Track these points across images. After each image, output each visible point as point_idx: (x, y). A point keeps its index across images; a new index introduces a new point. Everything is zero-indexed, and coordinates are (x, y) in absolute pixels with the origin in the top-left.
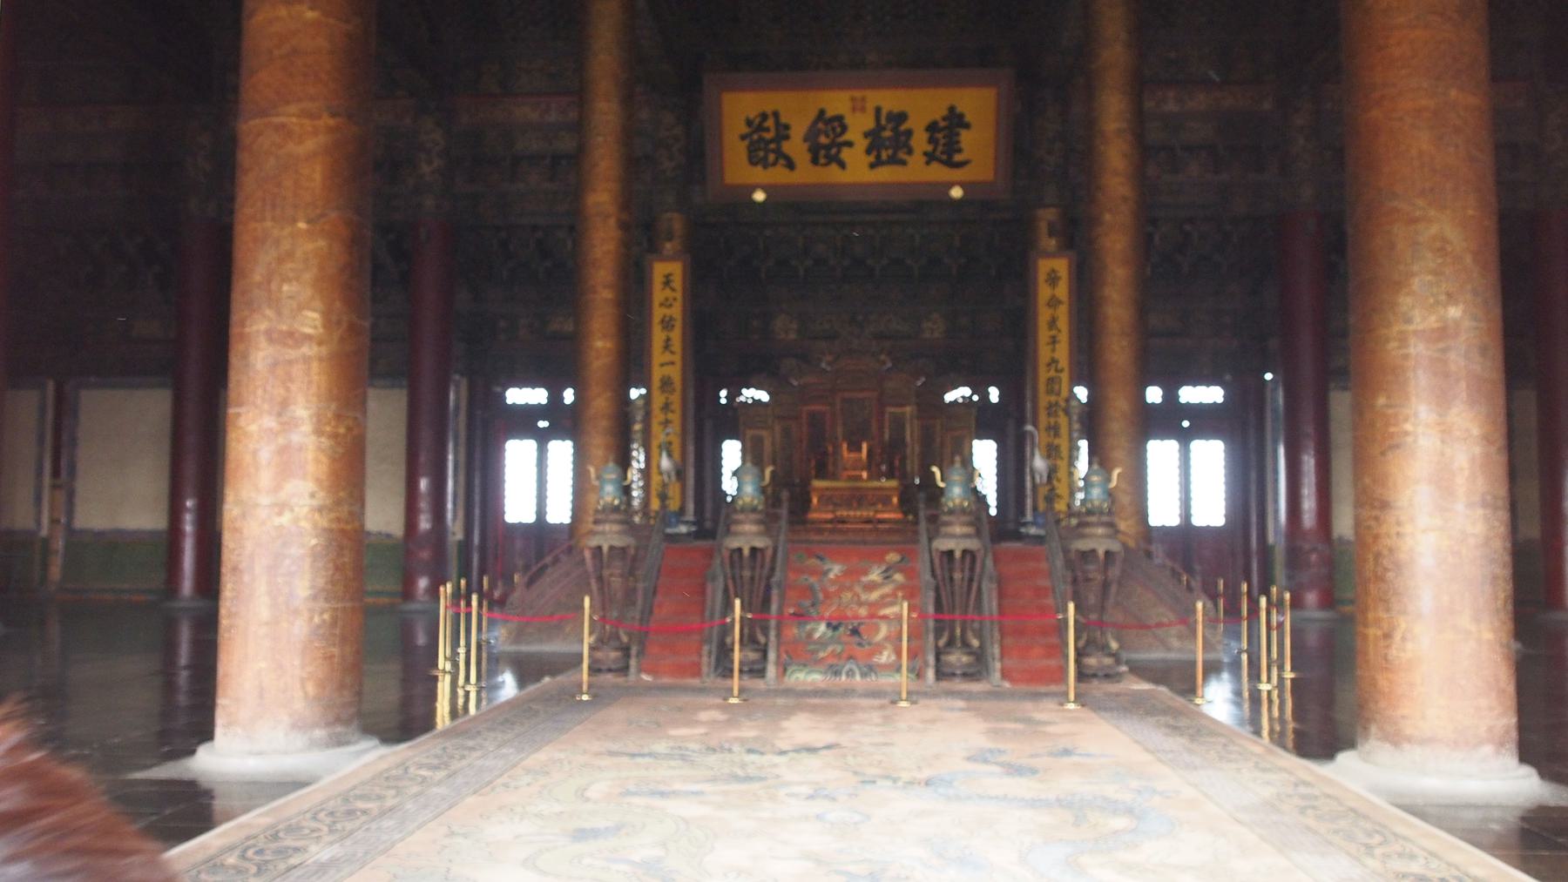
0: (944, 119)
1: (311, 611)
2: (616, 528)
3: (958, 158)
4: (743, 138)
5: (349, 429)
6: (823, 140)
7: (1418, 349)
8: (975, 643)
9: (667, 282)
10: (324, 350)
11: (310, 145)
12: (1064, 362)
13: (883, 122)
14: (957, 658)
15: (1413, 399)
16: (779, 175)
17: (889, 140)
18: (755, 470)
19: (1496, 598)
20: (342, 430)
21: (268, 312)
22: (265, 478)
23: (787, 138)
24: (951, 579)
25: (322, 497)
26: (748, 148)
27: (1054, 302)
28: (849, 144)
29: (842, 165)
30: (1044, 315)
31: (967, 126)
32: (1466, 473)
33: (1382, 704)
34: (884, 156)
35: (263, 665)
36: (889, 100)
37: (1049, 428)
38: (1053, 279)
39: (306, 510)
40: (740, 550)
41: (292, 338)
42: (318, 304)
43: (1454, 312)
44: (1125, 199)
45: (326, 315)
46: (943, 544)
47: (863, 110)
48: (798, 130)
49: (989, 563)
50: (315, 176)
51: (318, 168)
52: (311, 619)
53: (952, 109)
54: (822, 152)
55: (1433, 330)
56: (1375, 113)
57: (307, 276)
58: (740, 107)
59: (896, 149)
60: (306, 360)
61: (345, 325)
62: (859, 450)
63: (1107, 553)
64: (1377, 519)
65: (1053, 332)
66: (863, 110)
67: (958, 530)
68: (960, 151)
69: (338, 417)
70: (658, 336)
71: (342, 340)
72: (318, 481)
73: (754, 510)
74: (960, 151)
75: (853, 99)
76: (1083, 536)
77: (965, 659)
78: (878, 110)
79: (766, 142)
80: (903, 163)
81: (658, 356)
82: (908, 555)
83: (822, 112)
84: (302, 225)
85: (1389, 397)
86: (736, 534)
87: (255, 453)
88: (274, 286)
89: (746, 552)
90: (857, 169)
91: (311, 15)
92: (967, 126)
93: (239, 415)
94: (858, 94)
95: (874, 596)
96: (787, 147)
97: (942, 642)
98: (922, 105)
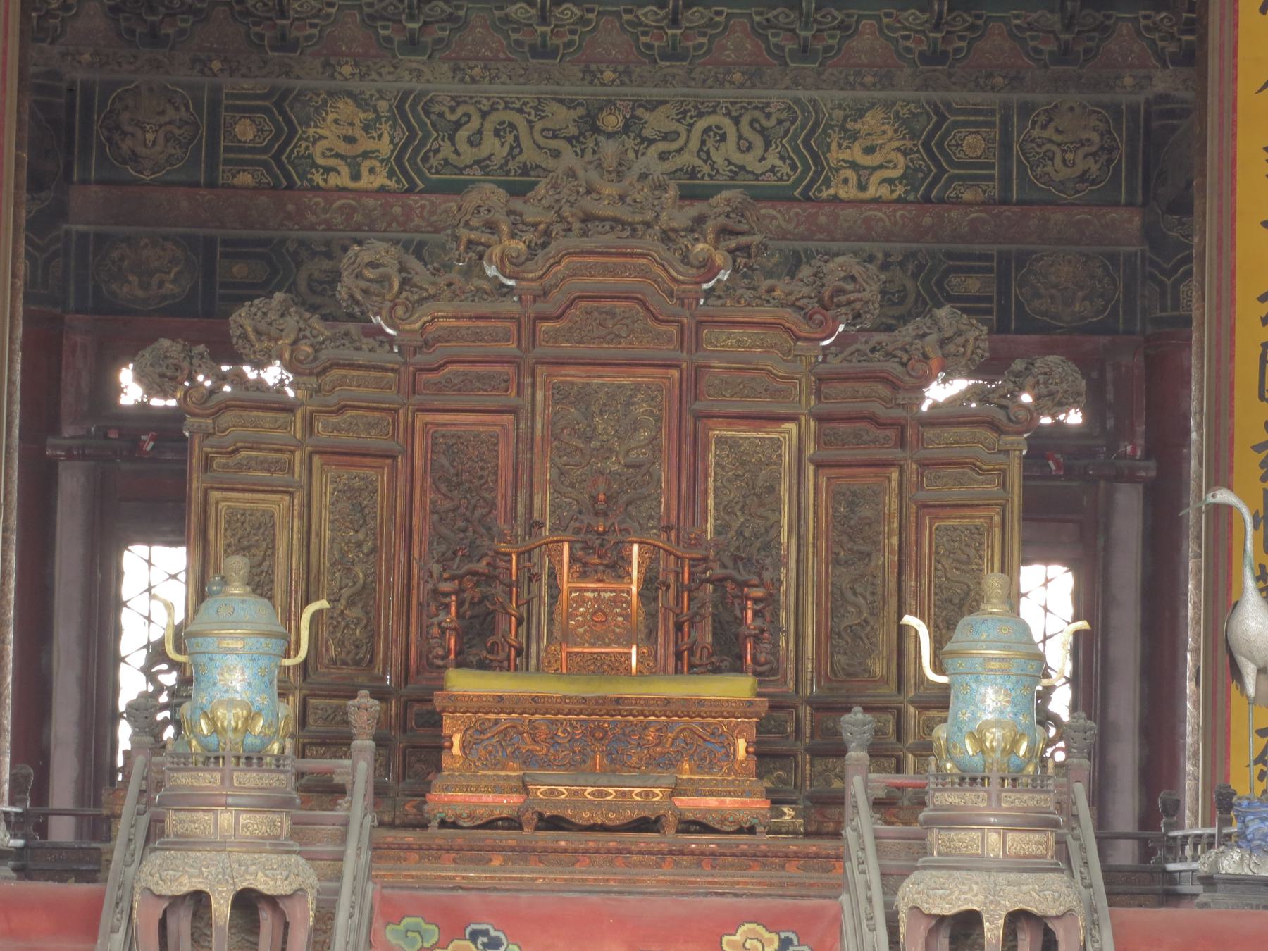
40: (199, 900)
62: (618, 567)
73: (253, 759)
86: (186, 843)
89: (221, 909)
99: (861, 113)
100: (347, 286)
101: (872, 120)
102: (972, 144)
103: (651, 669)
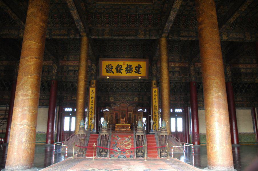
0: (138, 66)
1: (25, 144)
2: (83, 131)
3: (140, 72)
4: (105, 68)
5: (35, 111)
6: (118, 69)
7: (215, 100)
8: (143, 151)
9: (92, 91)
10: (31, 98)
11: (32, 63)
12: (157, 105)
14: (140, 154)
15: (214, 108)
16: (111, 74)
17: (129, 69)
18: (106, 121)
19: (229, 141)
20: (33, 112)
21: (22, 91)
22: (19, 119)
23: (113, 68)
24: (139, 140)
25: (29, 123)
27: (155, 95)
28: (123, 70)
29: (121, 73)
30: (154, 97)
31: (141, 67)
32: (223, 120)
33: (212, 159)
34: (128, 72)
35: (16, 154)
36: (129, 63)
37: (155, 116)
38: (155, 92)
39: (26, 125)
40: (103, 135)
41: (26, 95)
42: (31, 90)
43: (220, 94)
44: (166, 78)
45: (32, 91)
46: (138, 134)
47: (125, 64)
48: (114, 68)
49: (145, 137)
50: (32, 68)
51: (33, 67)
52: (25, 145)
53: (139, 65)
55: (217, 97)
56: (206, 63)
57: (29, 85)
58: (105, 63)
59: (130, 71)
60: (28, 99)
61: (35, 93)
62: (124, 119)
63: (165, 135)
64: (210, 128)
65: (155, 100)
66: (125, 64)
67: (140, 132)
69: (33, 109)
70: (91, 100)
71: (34, 96)
72: (28, 120)
73: (106, 128)
75: (123, 63)
76: (162, 133)
77: (141, 154)
78: (127, 64)
79: (109, 69)
81: (90, 103)
82: (132, 136)
83: (118, 65)
84: (29, 76)
85: (210, 108)
87: (17, 115)
88: (23, 86)
89: (104, 135)
90: (124, 74)
91: (34, 42)
92: (141, 67)
93: (15, 108)
94: (124, 62)
95: (126, 143)
96: (112, 70)
97: (137, 151)
98: (134, 64)
99: (135, 97)
100: (111, 106)
101: (136, 97)
102: (141, 98)
103: (126, 123)
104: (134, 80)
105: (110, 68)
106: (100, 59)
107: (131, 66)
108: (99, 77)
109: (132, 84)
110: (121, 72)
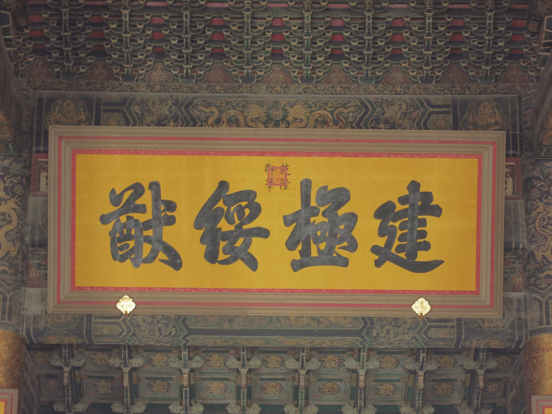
0: (403, 200)
3: (422, 256)
4: (104, 219)
6: (224, 225)
13: (313, 203)
23: (171, 221)
26: (112, 234)
28: (264, 233)
29: (252, 263)
31: (437, 211)
34: (314, 253)
36: (324, 172)
47: (284, 184)
48: (186, 214)
53: (414, 186)
54: (223, 244)
66: (284, 184)
68: (426, 246)
74: (426, 246)
75: (269, 168)
78: (306, 185)
80: (345, 263)
83: (223, 185)
90: (272, 270)
92: (437, 211)
94: (276, 161)
96: (169, 234)
98: (371, 179)
104: (369, 322)
105: (142, 218)
106: (54, 131)
107: (340, 196)
108: (44, 299)
109: (351, 363)
110: (252, 250)
